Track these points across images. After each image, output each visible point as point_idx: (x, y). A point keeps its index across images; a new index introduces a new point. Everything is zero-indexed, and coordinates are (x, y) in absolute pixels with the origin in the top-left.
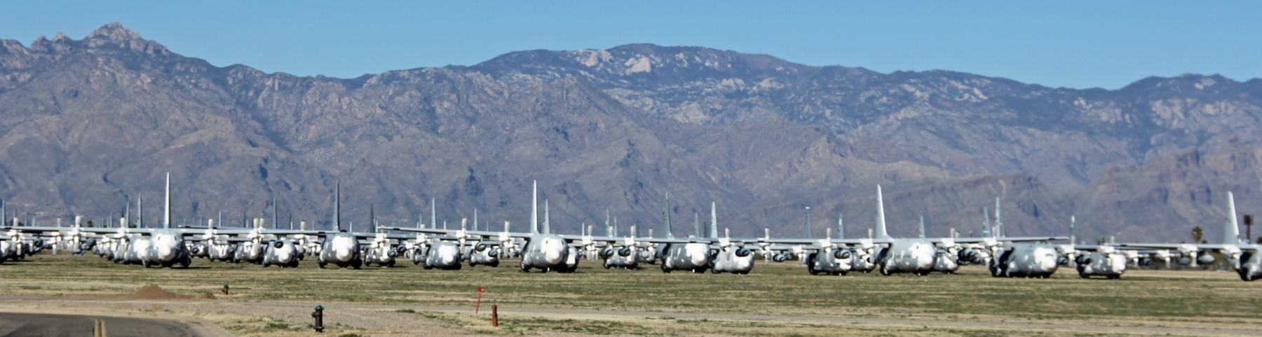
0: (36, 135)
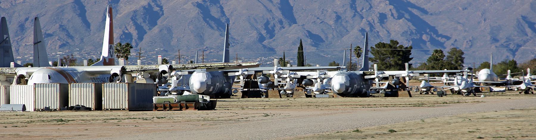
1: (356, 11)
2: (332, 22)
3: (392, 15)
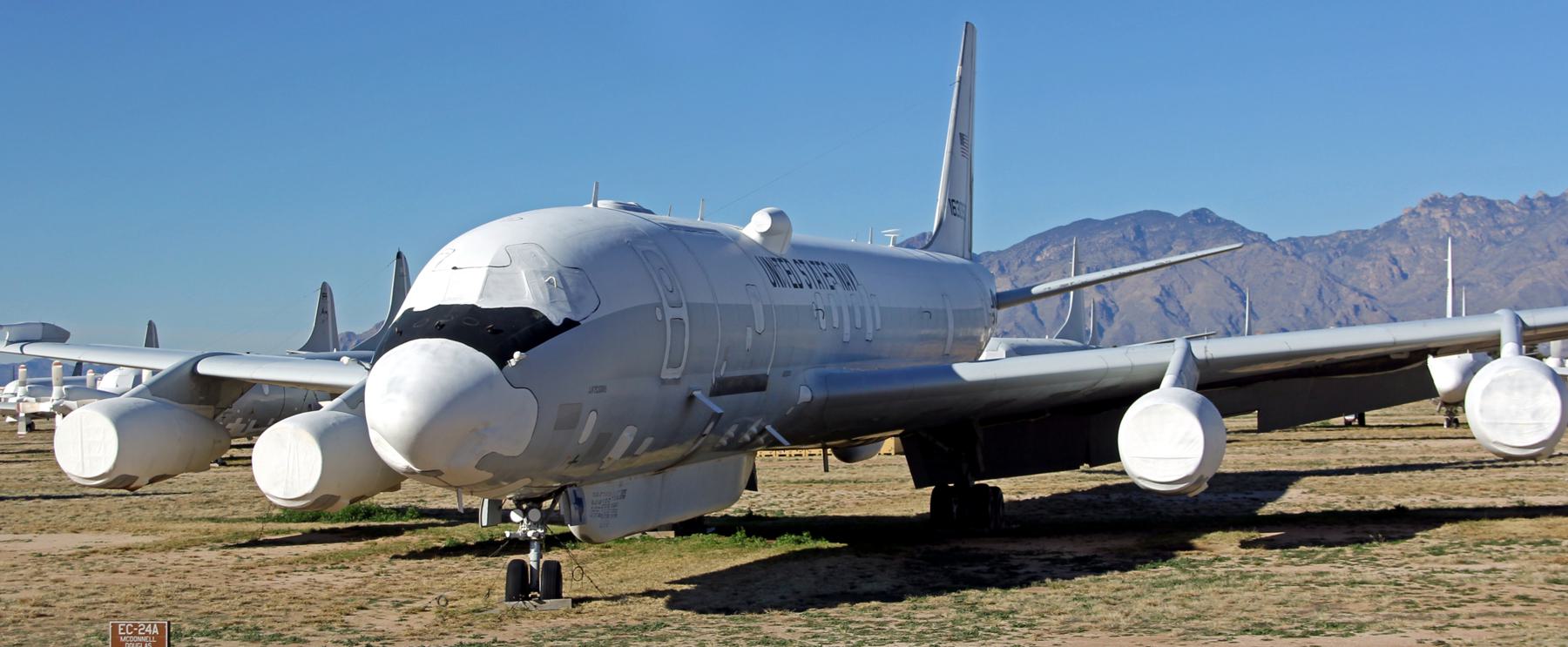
0: (1542, 279)
1: (1324, 304)
2: (1301, 315)
3: (1367, 306)
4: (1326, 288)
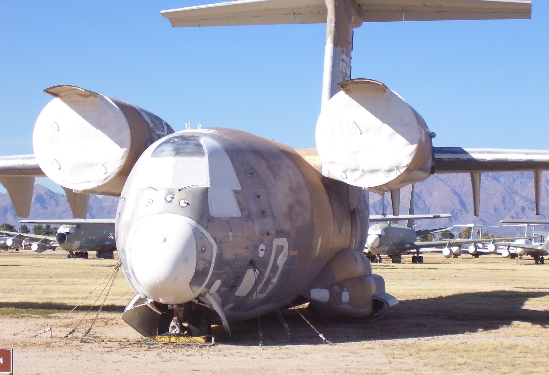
1: (505, 204)
2: (492, 212)
3: (529, 208)
4: (507, 196)
